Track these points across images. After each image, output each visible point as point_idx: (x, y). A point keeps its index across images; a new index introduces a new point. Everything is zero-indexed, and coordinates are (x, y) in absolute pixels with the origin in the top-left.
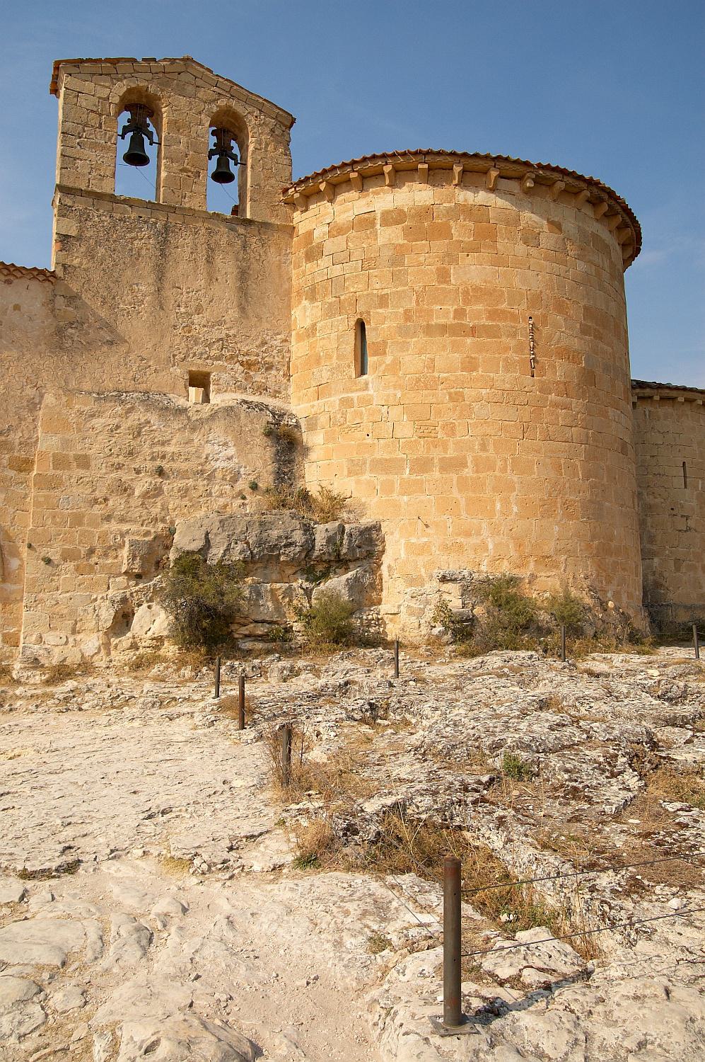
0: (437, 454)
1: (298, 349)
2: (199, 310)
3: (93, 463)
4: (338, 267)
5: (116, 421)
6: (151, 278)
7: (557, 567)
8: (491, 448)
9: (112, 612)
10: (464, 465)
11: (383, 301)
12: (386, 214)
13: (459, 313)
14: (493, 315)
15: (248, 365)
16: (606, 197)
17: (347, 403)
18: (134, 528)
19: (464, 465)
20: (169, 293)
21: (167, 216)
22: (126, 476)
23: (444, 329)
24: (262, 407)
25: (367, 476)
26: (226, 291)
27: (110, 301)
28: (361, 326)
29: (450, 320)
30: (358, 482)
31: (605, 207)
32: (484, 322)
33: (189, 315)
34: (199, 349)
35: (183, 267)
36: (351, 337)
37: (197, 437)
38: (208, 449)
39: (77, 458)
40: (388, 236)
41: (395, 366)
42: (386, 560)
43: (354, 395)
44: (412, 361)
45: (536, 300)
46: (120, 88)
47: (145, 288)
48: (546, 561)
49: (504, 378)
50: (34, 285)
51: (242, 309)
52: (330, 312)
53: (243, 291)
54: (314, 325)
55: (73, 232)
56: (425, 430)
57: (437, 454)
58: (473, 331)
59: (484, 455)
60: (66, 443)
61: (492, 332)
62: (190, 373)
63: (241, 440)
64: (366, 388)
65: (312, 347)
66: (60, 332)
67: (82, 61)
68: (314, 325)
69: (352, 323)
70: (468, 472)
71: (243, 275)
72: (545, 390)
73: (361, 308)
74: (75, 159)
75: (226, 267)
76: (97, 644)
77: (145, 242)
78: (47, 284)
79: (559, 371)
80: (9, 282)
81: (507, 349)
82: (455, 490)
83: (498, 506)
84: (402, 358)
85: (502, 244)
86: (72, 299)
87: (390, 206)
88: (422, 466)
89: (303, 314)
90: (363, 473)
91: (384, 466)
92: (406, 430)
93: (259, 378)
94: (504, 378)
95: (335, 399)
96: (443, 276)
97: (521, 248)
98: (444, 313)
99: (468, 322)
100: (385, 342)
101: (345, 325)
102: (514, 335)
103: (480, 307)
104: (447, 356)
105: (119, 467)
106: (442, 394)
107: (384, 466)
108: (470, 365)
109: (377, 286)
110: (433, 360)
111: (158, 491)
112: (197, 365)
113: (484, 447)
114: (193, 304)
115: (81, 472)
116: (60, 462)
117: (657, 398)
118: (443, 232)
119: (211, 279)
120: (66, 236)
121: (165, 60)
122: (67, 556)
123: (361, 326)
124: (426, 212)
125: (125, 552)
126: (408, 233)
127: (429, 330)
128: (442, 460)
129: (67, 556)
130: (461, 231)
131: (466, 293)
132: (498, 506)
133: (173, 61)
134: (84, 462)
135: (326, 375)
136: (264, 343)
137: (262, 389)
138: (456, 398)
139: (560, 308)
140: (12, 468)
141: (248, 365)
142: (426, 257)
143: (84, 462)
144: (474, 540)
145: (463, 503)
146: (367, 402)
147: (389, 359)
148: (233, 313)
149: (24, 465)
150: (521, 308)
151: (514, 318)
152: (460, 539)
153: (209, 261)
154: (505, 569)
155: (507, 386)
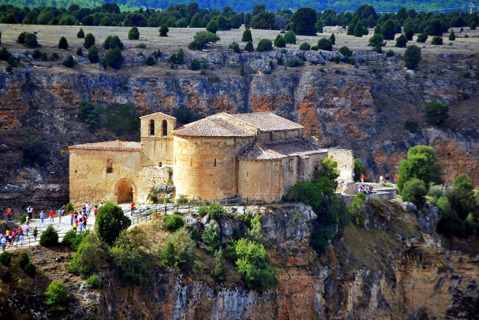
14: (187, 158)
20: (156, 151)
21: (156, 140)
27: (148, 153)
45: (192, 155)
47: (153, 150)
48: (191, 193)
49: (187, 167)
58: (184, 160)
61: (186, 160)
63: (164, 173)
66: (142, 158)
71: (166, 146)
72: (193, 169)
75: (164, 145)
79: (195, 165)
86: (143, 153)
93: (169, 162)
94: (187, 167)
108: (183, 165)
119: (162, 148)
130: (183, 145)
134: (145, 176)
137: (169, 164)
139: (196, 156)
143: (145, 176)
148: (165, 153)
149: (138, 177)
150: (190, 157)
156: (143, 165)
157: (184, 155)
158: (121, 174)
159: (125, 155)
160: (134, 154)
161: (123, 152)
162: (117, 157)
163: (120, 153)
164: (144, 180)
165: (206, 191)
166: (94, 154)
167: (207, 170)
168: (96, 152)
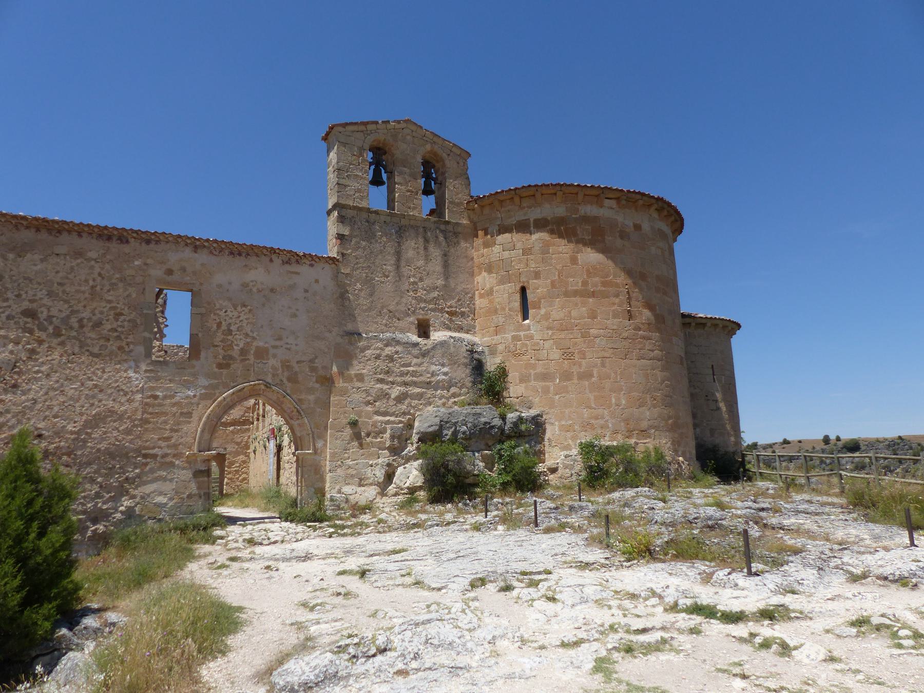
0: (575, 369)
1: (479, 302)
2: (421, 280)
3: (366, 378)
4: (507, 252)
5: (378, 352)
6: (393, 261)
7: (650, 437)
8: (607, 365)
9: (383, 471)
10: (592, 376)
11: (537, 275)
12: (535, 220)
13: (585, 283)
15: (451, 314)
16: (666, 206)
17: (516, 338)
18: (392, 419)
19: (592, 376)
20: (405, 271)
23: (576, 293)
25: (533, 383)
26: (436, 265)
28: (523, 290)
29: (579, 287)
30: (526, 388)
31: (665, 213)
32: (600, 288)
33: (415, 283)
34: (423, 305)
35: (410, 253)
36: (518, 297)
37: (427, 359)
38: (433, 368)
39: (356, 375)
41: (547, 317)
42: (548, 435)
43: (522, 333)
44: (557, 314)
46: (370, 140)
50: (327, 266)
51: (447, 277)
52: (501, 282)
53: (446, 265)
54: (491, 289)
55: (347, 233)
56: (567, 355)
58: (593, 295)
59: (604, 370)
61: (605, 295)
62: (418, 320)
64: (529, 329)
65: (491, 302)
67: (347, 124)
68: (491, 289)
69: (518, 288)
73: (523, 279)
74: (346, 186)
76: (375, 493)
78: (333, 266)
80: (312, 265)
81: (614, 304)
82: (587, 391)
83: (613, 400)
84: (551, 310)
85: (608, 239)
87: (539, 216)
88: (566, 376)
89: (484, 280)
90: (530, 381)
91: (545, 377)
92: (556, 354)
93: (458, 321)
95: (509, 336)
96: (574, 260)
97: (619, 242)
98: (575, 283)
100: (540, 302)
101: (513, 288)
102: (617, 296)
103: (597, 279)
104: (579, 310)
108: (593, 316)
109: (533, 266)
110: (570, 312)
113: (603, 365)
114: (418, 275)
115: (359, 384)
117: (693, 324)
119: (427, 259)
120: (343, 235)
121: (394, 121)
123: (523, 290)
125: (387, 435)
127: (567, 294)
128: (578, 373)
131: (588, 271)
132: (613, 400)
133: (399, 122)
135: (501, 320)
136: (459, 300)
137: (460, 329)
140: (317, 382)
141: (451, 314)
144: (602, 422)
145: (592, 398)
146: (531, 337)
147: (543, 311)
148: (440, 282)
151: (617, 285)
152: (593, 421)
153: (426, 248)
155: (615, 327)
157: (591, 271)
158: (237, 367)
159: (259, 275)
160: (306, 272)
161: (253, 260)
162: (219, 278)
163: (239, 261)
164: (358, 397)
166: (79, 254)
168: (94, 249)
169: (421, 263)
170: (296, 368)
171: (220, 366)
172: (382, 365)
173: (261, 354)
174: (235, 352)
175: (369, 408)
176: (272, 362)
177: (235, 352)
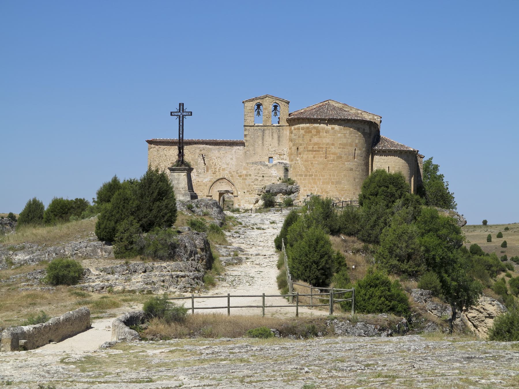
11: (301, 145)
13: (313, 148)
14: (319, 148)
17: (295, 163)
22: (257, 177)
23: (310, 151)
24: (282, 163)
35: (267, 137)
37: (270, 170)
40: (302, 132)
42: (300, 192)
44: (305, 157)
47: (260, 142)
51: (279, 144)
53: (279, 140)
57: (308, 174)
58: (315, 151)
60: (247, 172)
61: (318, 151)
70: (313, 177)
71: (279, 137)
75: (276, 136)
77: (260, 133)
85: (321, 134)
88: (306, 176)
91: (301, 175)
92: (304, 169)
93: (282, 157)
96: (310, 140)
97: (325, 134)
98: (310, 148)
99: (314, 149)
105: (256, 176)
106: (310, 163)
107: (301, 175)
108: (314, 157)
111: (263, 180)
112: (270, 156)
116: (246, 175)
118: (310, 132)
119: (272, 138)
122: (248, 191)
123: (298, 148)
124: (308, 128)
126: (305, 132)
127: (308, 151)
129: (248, 191)
138: (312, 163)
142: (308, 137)
143: (250, 175)
148: (277, 145)
151: (323, 148)
154: (319, 194)
156: (248, 161)
157: (315, 144)
158: (217, 173)
165: (346, 190)
167: (346, 163)
169: (270, 140)
170: (233, 173)
171: (213, 173)
172: (257, 171)
173: (224, 170)
174: (217, 170)
175: (252, 184)
176: (226, 172)
177: (217, 170)
